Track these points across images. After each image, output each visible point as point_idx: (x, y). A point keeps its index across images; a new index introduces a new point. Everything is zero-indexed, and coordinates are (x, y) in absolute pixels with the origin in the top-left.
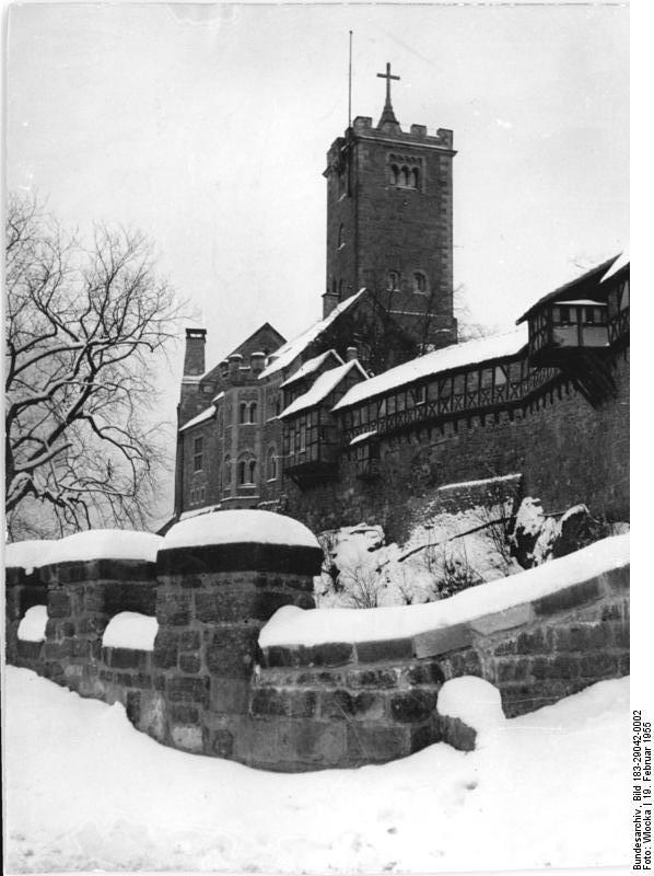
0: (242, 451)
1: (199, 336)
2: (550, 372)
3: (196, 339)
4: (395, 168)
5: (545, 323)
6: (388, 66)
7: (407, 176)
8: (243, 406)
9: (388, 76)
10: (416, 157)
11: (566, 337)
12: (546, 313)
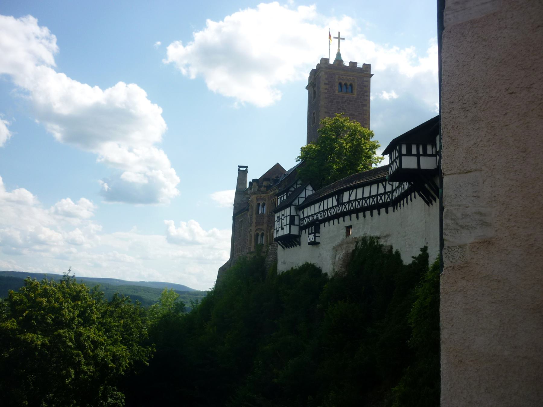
0: (259, 227)
1: (245, 169)
2: (406, 186)
3: (243, 172)
4: (340, 84)
5: (397, 155)
6: (339, 33)
7: (347, 88)
8: (259, 204)
9: (339, 38)
10: (352, 78)
11: (409, 163)
12: (398, 148)
